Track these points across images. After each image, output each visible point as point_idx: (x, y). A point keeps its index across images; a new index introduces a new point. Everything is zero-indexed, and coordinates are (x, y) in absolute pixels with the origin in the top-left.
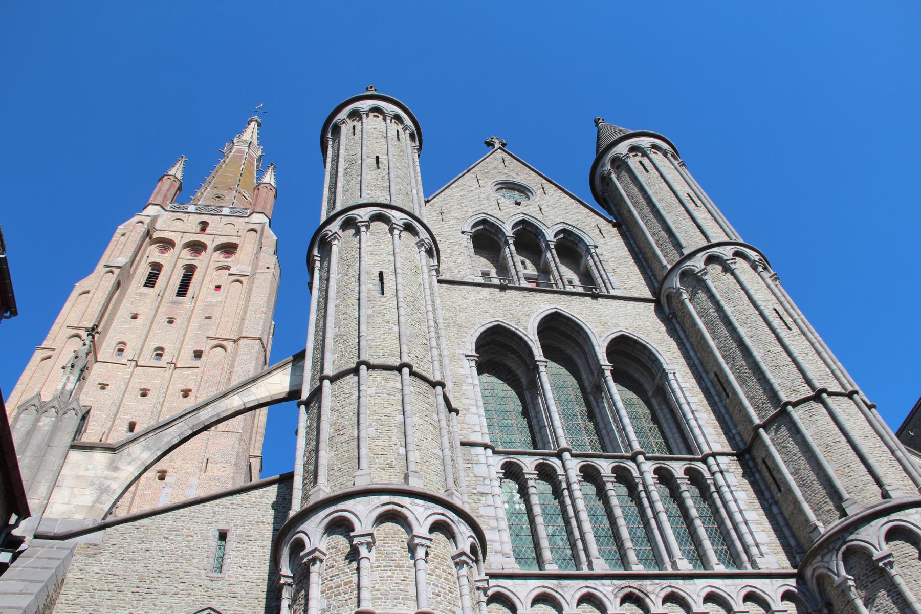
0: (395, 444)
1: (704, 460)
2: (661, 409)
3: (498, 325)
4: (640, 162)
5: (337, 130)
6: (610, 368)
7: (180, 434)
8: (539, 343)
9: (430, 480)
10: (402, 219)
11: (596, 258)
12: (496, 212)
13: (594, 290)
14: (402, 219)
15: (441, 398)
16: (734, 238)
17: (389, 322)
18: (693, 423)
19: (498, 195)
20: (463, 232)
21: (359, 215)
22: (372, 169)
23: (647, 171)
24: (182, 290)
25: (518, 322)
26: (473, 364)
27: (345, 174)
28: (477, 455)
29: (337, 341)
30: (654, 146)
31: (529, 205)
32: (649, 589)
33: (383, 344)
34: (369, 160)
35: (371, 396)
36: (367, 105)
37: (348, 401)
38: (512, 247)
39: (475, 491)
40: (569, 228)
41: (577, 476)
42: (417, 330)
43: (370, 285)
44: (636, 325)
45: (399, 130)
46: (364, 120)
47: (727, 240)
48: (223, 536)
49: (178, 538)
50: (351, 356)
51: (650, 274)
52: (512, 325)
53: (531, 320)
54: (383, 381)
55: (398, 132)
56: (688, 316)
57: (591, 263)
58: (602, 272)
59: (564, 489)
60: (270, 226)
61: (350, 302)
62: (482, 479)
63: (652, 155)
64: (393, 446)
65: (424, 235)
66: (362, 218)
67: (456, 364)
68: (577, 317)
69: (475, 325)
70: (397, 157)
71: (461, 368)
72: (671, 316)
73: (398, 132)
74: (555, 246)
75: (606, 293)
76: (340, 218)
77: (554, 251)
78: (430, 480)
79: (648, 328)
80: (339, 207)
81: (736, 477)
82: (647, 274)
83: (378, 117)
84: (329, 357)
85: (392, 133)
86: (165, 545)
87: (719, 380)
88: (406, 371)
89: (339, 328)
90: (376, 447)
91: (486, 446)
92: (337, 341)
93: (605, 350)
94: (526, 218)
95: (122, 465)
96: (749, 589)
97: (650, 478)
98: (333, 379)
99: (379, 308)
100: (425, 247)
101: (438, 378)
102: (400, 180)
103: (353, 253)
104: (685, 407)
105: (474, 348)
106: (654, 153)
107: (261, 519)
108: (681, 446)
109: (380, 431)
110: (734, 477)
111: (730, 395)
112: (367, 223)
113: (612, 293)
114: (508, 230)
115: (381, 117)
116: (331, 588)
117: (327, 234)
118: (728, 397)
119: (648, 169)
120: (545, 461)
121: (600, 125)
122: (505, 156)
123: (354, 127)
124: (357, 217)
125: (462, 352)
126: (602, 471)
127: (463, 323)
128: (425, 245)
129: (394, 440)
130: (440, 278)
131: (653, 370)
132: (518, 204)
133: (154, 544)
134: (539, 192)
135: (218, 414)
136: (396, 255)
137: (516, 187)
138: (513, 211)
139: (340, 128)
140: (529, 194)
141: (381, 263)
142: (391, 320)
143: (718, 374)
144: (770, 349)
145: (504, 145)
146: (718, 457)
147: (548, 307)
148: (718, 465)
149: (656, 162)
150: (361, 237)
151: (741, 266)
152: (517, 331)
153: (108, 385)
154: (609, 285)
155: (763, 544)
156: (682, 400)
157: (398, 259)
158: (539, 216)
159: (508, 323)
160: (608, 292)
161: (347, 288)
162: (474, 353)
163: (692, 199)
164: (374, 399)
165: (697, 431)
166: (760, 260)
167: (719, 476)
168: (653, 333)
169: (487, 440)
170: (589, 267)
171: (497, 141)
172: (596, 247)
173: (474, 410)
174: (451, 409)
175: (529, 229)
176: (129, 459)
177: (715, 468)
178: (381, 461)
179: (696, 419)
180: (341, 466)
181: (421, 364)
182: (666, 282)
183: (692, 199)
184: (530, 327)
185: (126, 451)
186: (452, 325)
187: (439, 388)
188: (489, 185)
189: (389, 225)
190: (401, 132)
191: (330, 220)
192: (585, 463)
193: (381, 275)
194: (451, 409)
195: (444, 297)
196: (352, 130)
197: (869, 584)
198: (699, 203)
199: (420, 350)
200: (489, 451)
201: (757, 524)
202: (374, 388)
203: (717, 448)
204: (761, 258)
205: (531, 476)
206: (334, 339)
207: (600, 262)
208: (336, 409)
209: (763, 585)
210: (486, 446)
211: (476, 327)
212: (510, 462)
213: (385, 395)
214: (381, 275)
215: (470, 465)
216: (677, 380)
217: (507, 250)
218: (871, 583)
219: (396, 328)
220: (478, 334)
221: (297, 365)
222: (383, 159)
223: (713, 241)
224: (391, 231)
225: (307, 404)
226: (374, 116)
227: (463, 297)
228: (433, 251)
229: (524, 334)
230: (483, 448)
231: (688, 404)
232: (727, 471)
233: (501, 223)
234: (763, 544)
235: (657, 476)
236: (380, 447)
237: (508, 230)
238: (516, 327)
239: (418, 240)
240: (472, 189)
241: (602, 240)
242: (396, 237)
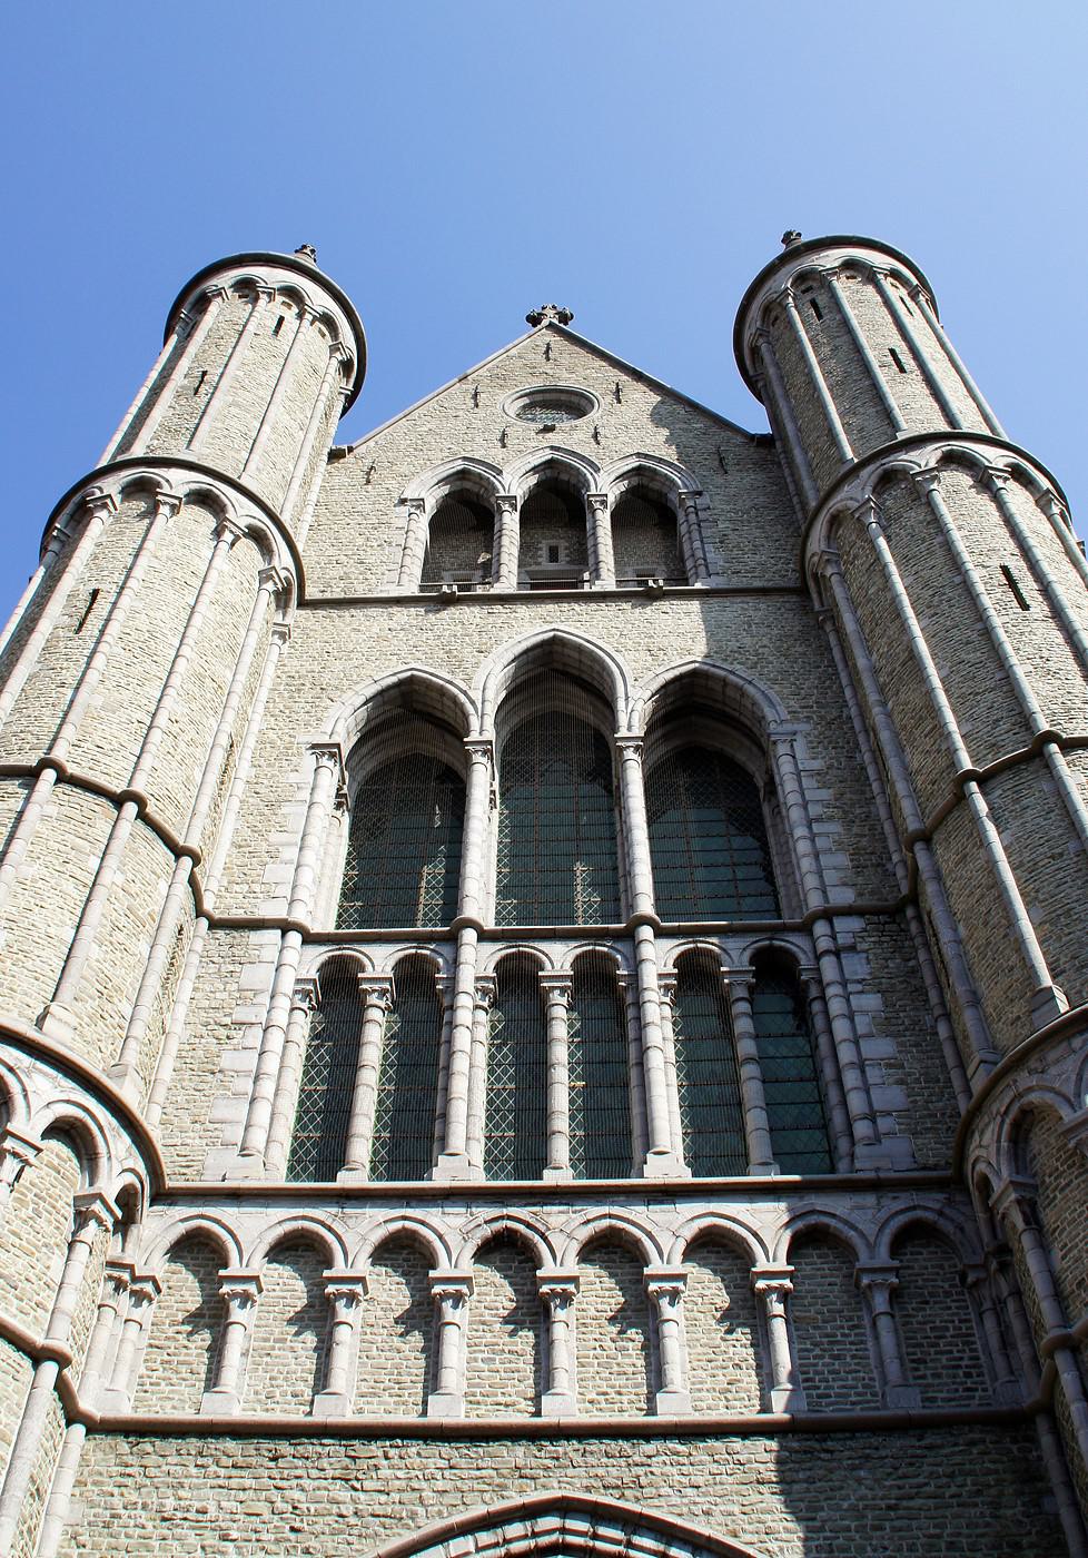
3: (412, 679)
9: (11, 989)
25: (457, 664)
30: (894, 274)
39: (227, 1020)
44: (734, 645)
62: (250, 994)
67: (285, 763)
68: (599, 643)
72: (821, 618)
81: (869, 963)
94: (558, 455)
96: (813, 1219)
99: (57, 659)
110: (864, 961)
112: (177, 502)
132: (548, 429)
137: (563, 397)
144: (964, 656)
145: (564, 318)
155: (889, 1114)
159: (432, 670)
168: (771, 658)
192: (514, 950)
195: (312, 634)
197: (1057, 1193)
201: (890, 1066)
209: (853, 1209)
215: (237, 968)
218: (1063, 1189)
229: (461, 690)
232: (852, 948)
234: (889, 1114)
238: (448, 677)
241: (719, 480)
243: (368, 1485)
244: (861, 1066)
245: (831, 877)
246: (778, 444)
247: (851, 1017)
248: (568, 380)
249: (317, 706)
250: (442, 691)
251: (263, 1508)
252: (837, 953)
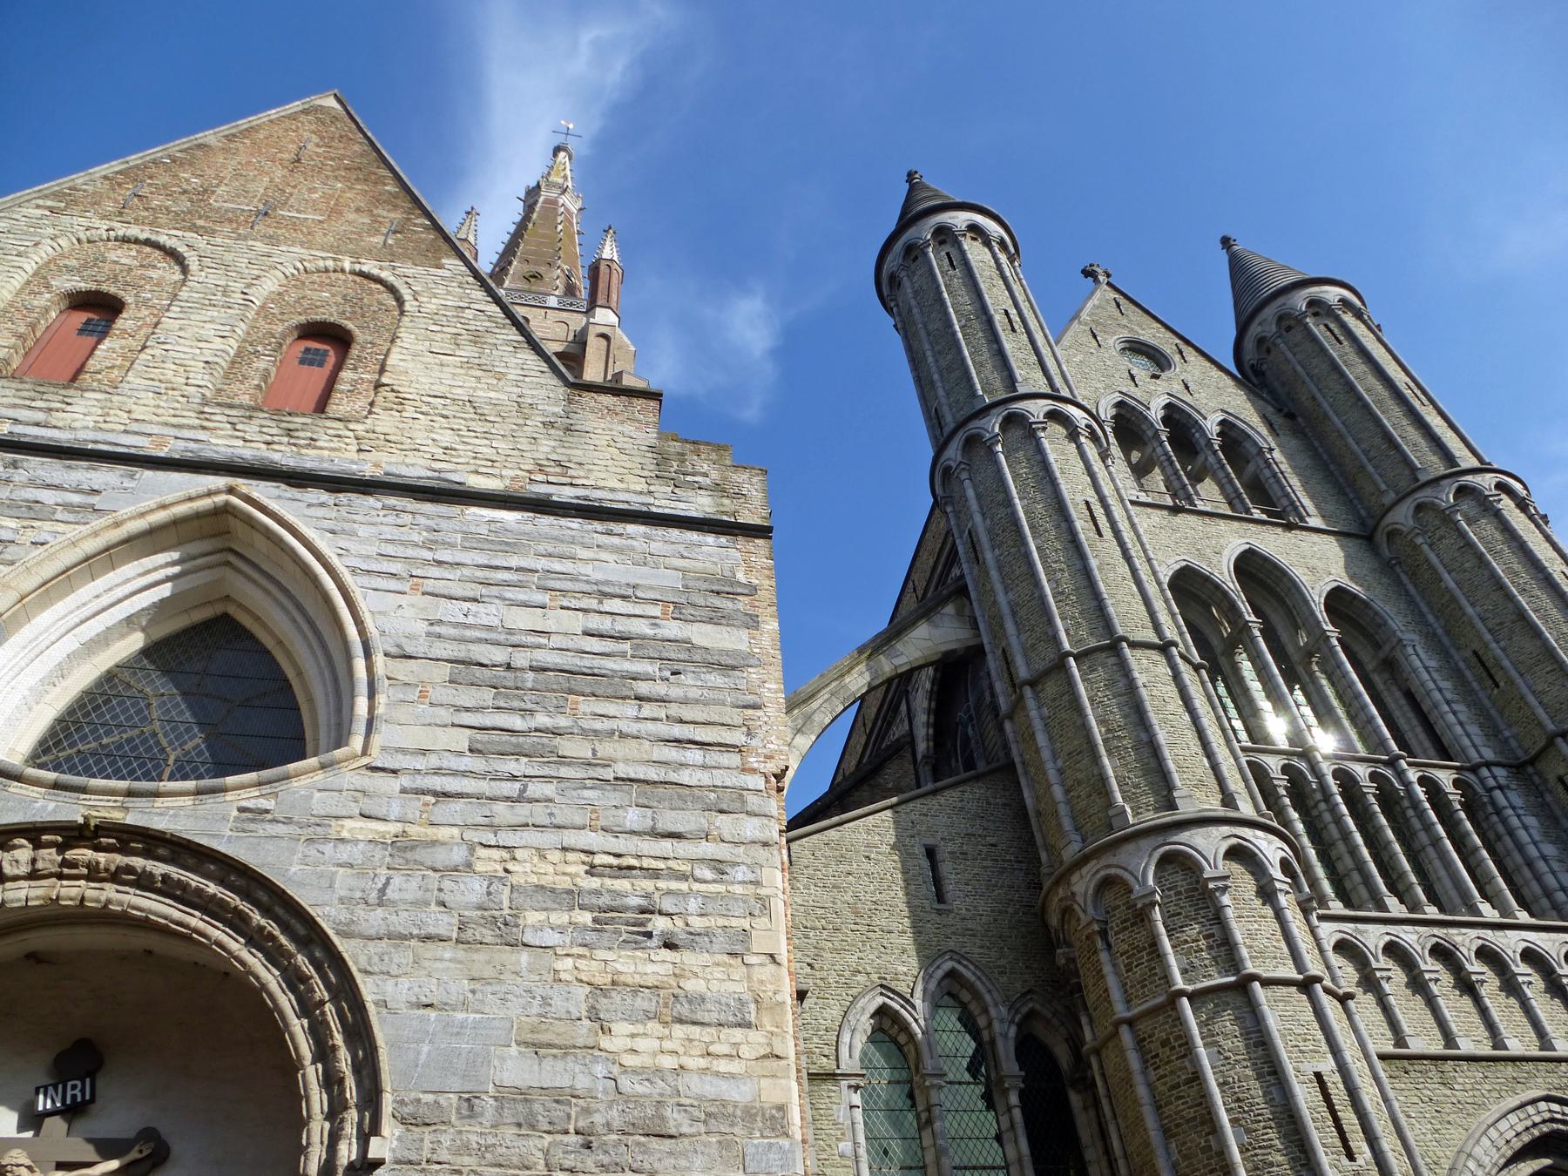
2: (1388, 690)
32: (1458, 939)
40: (1231, 419)
48: (931, 853)
49: (880, 857)
52: (1204, 567)
59: (1319, 801)
82: (1345, 494)
86: (866, 866)
107: (970, 830)
108: (1427, 744)
111: (1502, 684)
116: (1186, 942)
118: (1497, 686)
133: (855, 866)
137: (1144, 348)
147: (1239, 542)
148: (1495, 778)
158: (1187, 398)
167: (1498, 794)
175: (1176, 416)
182: (1390, 514)
189: (1067, 429)
203: (1489, 754)
205: (1281, 783)
216: (1418, 655)
232: (1508, 787)
243: (1456, 1087)
244: (1544, 858)
245: (1477, 740)
247: (1526, 828)
251: (1416, 1100)
252: (1500, 788)
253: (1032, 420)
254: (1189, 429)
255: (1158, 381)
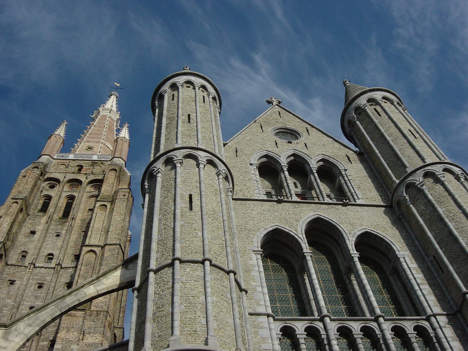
0: (199, 317)
1: (428, 319)
3: (277, 229)
4: (375, 109)
5: (162, 97)
6: (358, 255)
7: (52, 314)
8: (306, 240)
9: (224, 342)
10: (206, 157)
11: (346, 178)
12: (274, 149)
13: (344, 201)
14: (206, 157)
15: (234, 284)
16: (443, 159)
17: (196, 230)
18: (419, 293)
19: (276, 138)
20: (251, 164)
21: (175, 156)
22: (185, 123)
23: (380, 116)
24: (66, 214)
25: (291, 225)
26: (259, 257)
27: (167, 127)
28: (262, 323)
29: (159, 244)
31: (297, 143)
33: (191, 245)
34: (183, 117)
35: (183, 283)
36: (182, 79)
37: (166, 287)
38: (287, 173)
40: (327, 158)
41: (335, 334)
42: (216, 234)
43: (182, 204)
45: (205, 96)
46: (180, 90)
47: (438, 161)
50: (169, 255)
51: (385, 187)
52: (287, 228)
53: (300, 223)
54: (191, 272)
55: (204, 97)
56: (412, 216)
57: (343, 181)
58: (351, 188)
59: (326, 344)
60: (125, 167)
61: (168, 216)
63: (383, 104)
64: (198, 318)
65: (221, 167)
66: (177, 158)
68: (333, 220)
69: (260, 229)
70: (203, 114)
71: (250, 260)
72: (400, 217)
73: (204, 97)
74: (316, 171)
75: (354, 203)
76: (162, 158)
77: (316, 175)
78: (224, 342)
79: (384, 226)
80: (162, 152)
82: (383, 187)
83: (190, 87)
84: (154, 255)
85: (199, 98)
87: (437, 261)
88: (207, 263)
89: (161, 235)
90: (185, 319)
91: (268, 316)
92: (159, 244)
93: (353, 243)
95: (11, 337)
97: (389, 334)
98: (156, 272)
100: (222, 175)
101: (231, 268)
102: (204, 130)
103: (172, 182)
104: (413, 281)
105: (259, 245)
106: (385, 102)
108: (412, 309)
109: (188, 307)
111: (444, 272)
113: (358, 202)
114: (284, 161)
115: (192, 87)
117: (154, 170)
119: (381, 114)
120: (311, 325)
121: (347, 85)
122: (280, 110)
123: (173, 95)
124: (174, 157)
125: (251, 248)
126: (353, 330)
127: (253, 229)
128: (223, 174)
129: (199, 313)
130: (234, 197)
131: (389, 256)
134: (305, 134)
135: (79, 300)
136: (201, 182)
138: (287, 147)
139: (164, 96)
140: (299, 136)
141: (191, 188)
142: (197, 228)
143: (435, 256)
145: (279, 102)
146: (437, 317)
147: (312, 214)
149: (386, 108)
150: (177, 171)
151: (448, 178)
152: (290, 232)
153: (15, 281)
154: (355, 196)
156: (411, 277)
157: (203, 185)
160: (355, 202)
161: (167, 206)
162: (260, 249)
163: (412, 133)
164: (185, 285)
165: (422, 298)
166: (462, 173)
169: (270, 311)
170: (341, 185)
171: (275, 100)
172: (346, 170)
173: (259, 289)
174: (241, 290)
175: (298, 160)
176: (16, 333)
177: (436, 325)
178: (189, 329)
179: (421, 290)
180: (160, 333)
181: (219, 258)
183: (412, 133)
184: (299, 230)
185: (14, 327)
186: (243, 229)
187: (232, 275)
188: (270, 130)
190: (206, 97)
191: (156, 160)
193: (190, 196)
194: (241, 290)
196: (172, 97)
198: (417, 135)
199: (218, 248)
200: (271, 319)
202: (185, 277)
204: (463, 172)
206: (157, 243)
207: (349, 181)
208: (158, 292)
210: (268, 316)
211: (261, 231)
212: (286, 326)
213: (193, 281)
214: (190, 196)
215: (257, 330)
216: (406, 263)
217: (283, 176)
219: (200, 234)
220: (263, 235)
221: (135, 262)
222: (193, 116)
223: (428, 161)
224: (198, 165)
225: (139, 290)
226: (188, 87)
227: (251, 210)
228: (229, 177)
229: (295, 234)
230: (266, 317)
231: (415, 279)
233: (278, 157)
235: (393, 333)
236: (188, 319)
237: (284, 161)
238: (290, 229)
239: (217, 171)
240: (257, 134)
241: (350, 165)
242: (202, 169)
246: (365, 155)
248: (291, 126)
249: (249, 237)
250: (288, 234)
253: (176, 159)
254: (304, 165)
255: (290, 145)
